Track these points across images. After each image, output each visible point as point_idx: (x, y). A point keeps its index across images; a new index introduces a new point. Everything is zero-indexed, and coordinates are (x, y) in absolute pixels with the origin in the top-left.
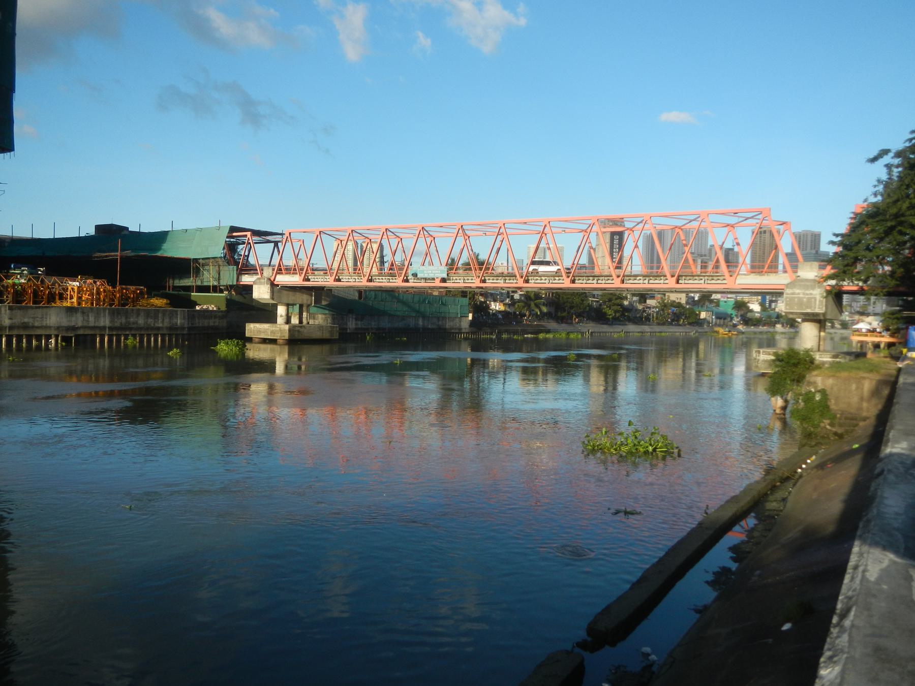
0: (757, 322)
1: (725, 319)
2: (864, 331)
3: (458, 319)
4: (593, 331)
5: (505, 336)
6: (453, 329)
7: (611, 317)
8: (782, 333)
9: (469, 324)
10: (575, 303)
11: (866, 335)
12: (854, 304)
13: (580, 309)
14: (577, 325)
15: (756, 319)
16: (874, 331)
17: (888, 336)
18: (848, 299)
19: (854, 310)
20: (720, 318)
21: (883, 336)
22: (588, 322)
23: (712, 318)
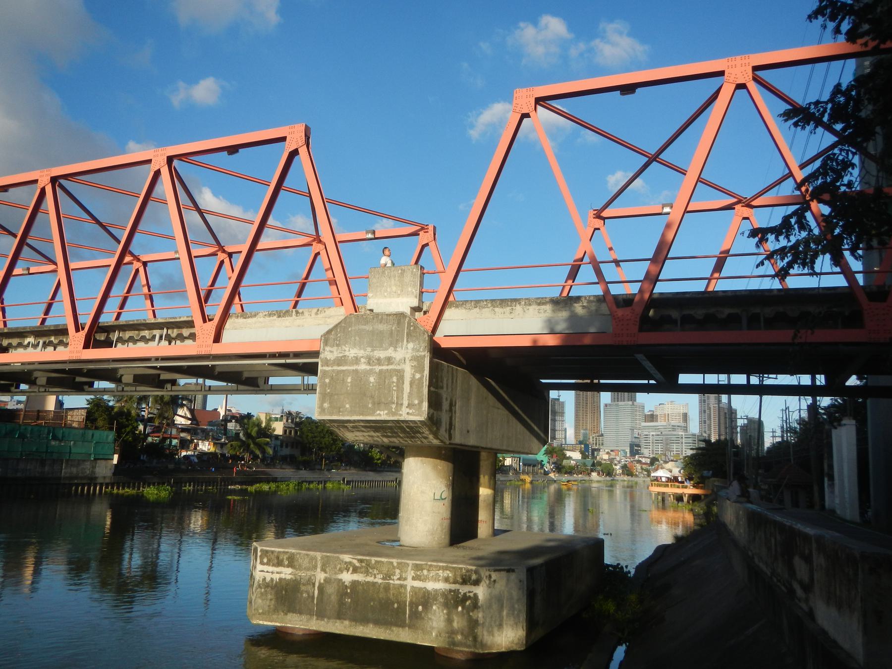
0: (570, 471)
1: (534, 466)
2: (664, 479)
3: (89, 463)
4: (349, 479)
5: (188, 488)
6: (76, 478)
7: (379, 462)
8: (598, 482)
9: (113, 471)
10: (323, 443)
11: (667, 486)
12: (668, 453)
13: (331, 451)
14: (326, 473)
15: (570, 466)
16: (675, 479)
17: (692, 487)
18: (662, 448)
19: (668, 459)
20: (529, 465)
21: (686, 487)
22: (348, 468)
23: (519, 464)
